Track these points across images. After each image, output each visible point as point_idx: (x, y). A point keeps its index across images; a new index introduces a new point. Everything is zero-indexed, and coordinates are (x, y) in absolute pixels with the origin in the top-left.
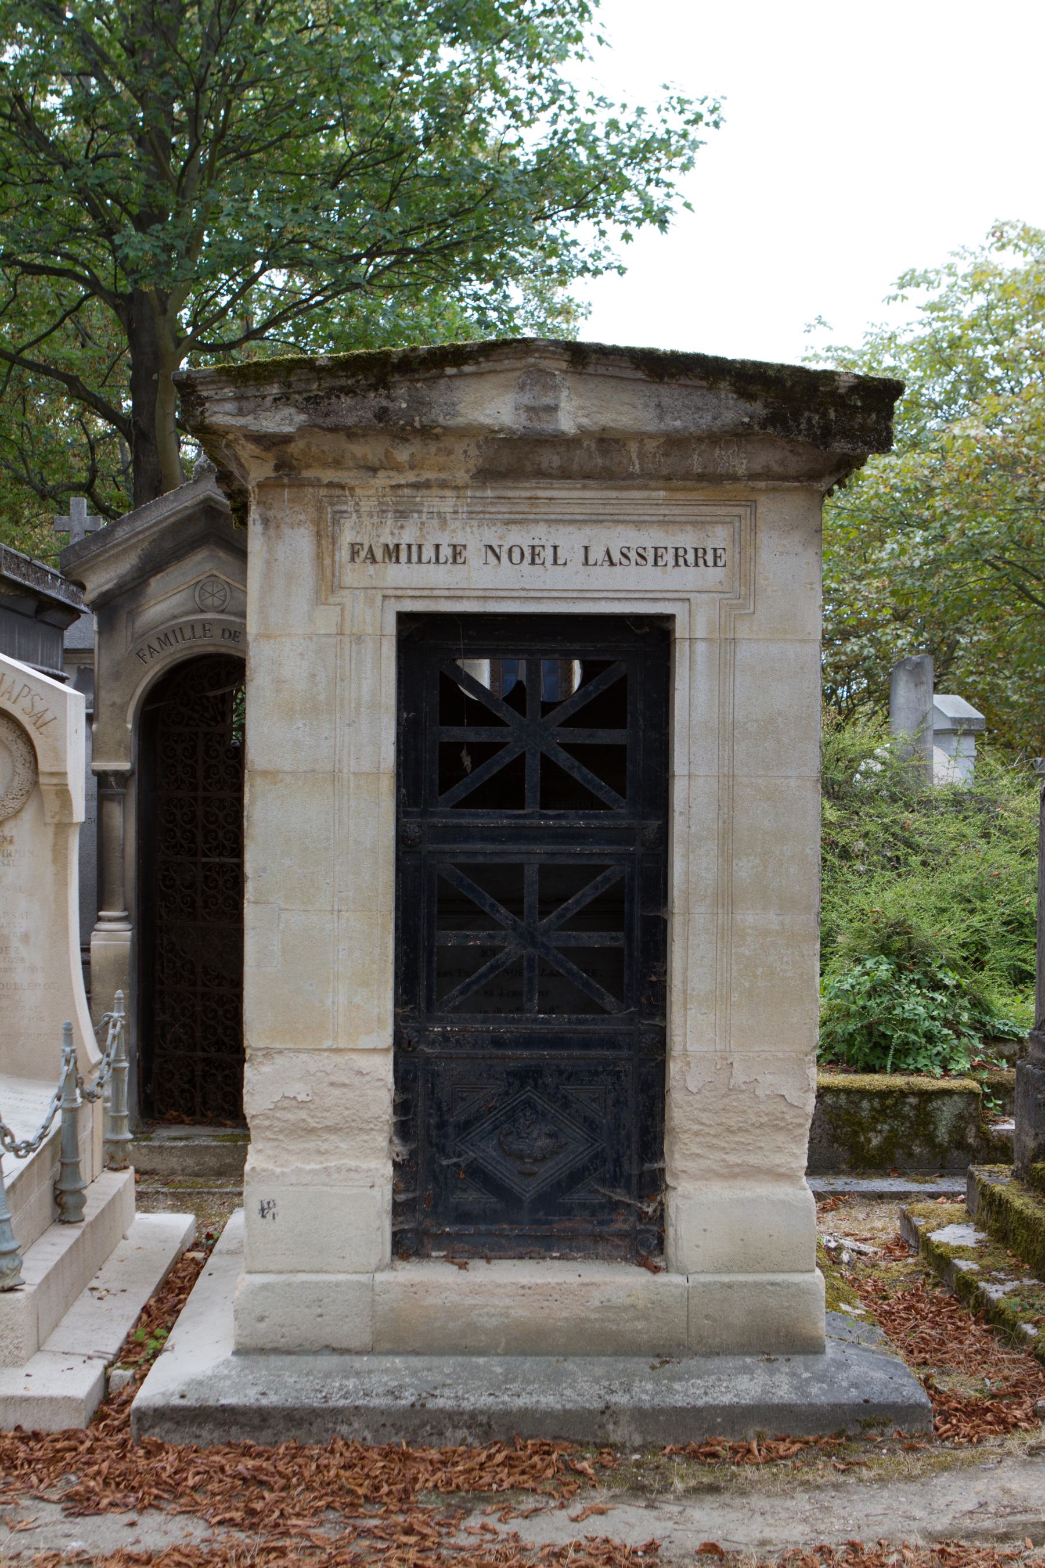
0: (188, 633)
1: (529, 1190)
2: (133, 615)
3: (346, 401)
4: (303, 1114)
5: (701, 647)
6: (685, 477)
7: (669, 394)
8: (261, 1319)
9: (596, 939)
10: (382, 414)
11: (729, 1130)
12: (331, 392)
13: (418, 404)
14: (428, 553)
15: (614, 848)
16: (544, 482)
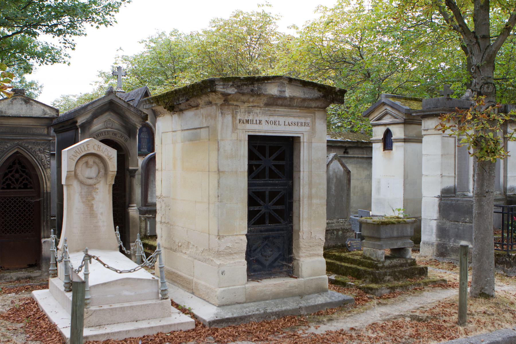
0: (104, 134)
1: (267, 263)
2: (89, 128)
3: (245, 87)
4: (230, 250)
5: (305, 144)
6: (303, 107)
7: (306, 90)
8: (223, 298)
9: (279, 207)
10: (252, 90)
11: (311, 247)
12: (242, 85)
13: (259, 89)
14: (255, 122)
15: (282, 187)
16: (278, 107)
